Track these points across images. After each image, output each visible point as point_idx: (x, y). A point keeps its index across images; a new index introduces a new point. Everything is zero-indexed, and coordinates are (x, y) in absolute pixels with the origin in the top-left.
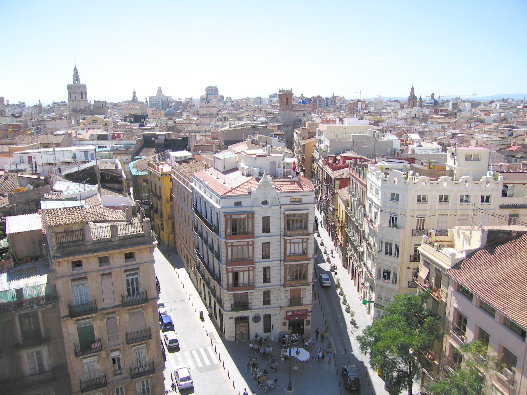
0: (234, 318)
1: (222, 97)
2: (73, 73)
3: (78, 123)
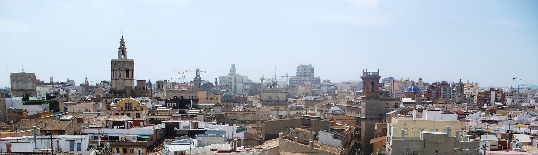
1: (318, 80)
3: (109, 108)
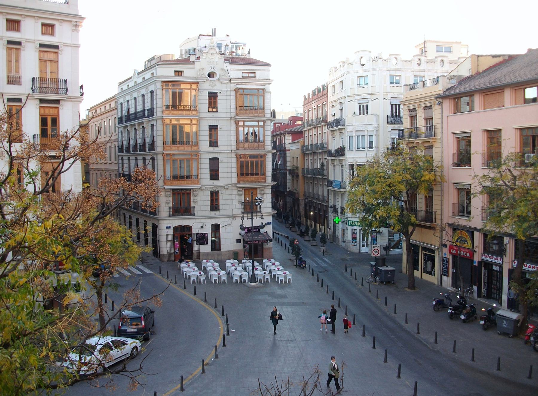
0: (172, 228)
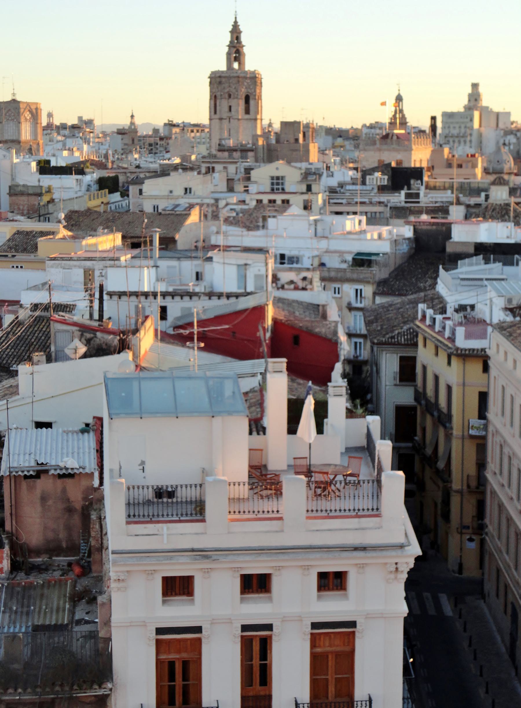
2: (227, 39)
